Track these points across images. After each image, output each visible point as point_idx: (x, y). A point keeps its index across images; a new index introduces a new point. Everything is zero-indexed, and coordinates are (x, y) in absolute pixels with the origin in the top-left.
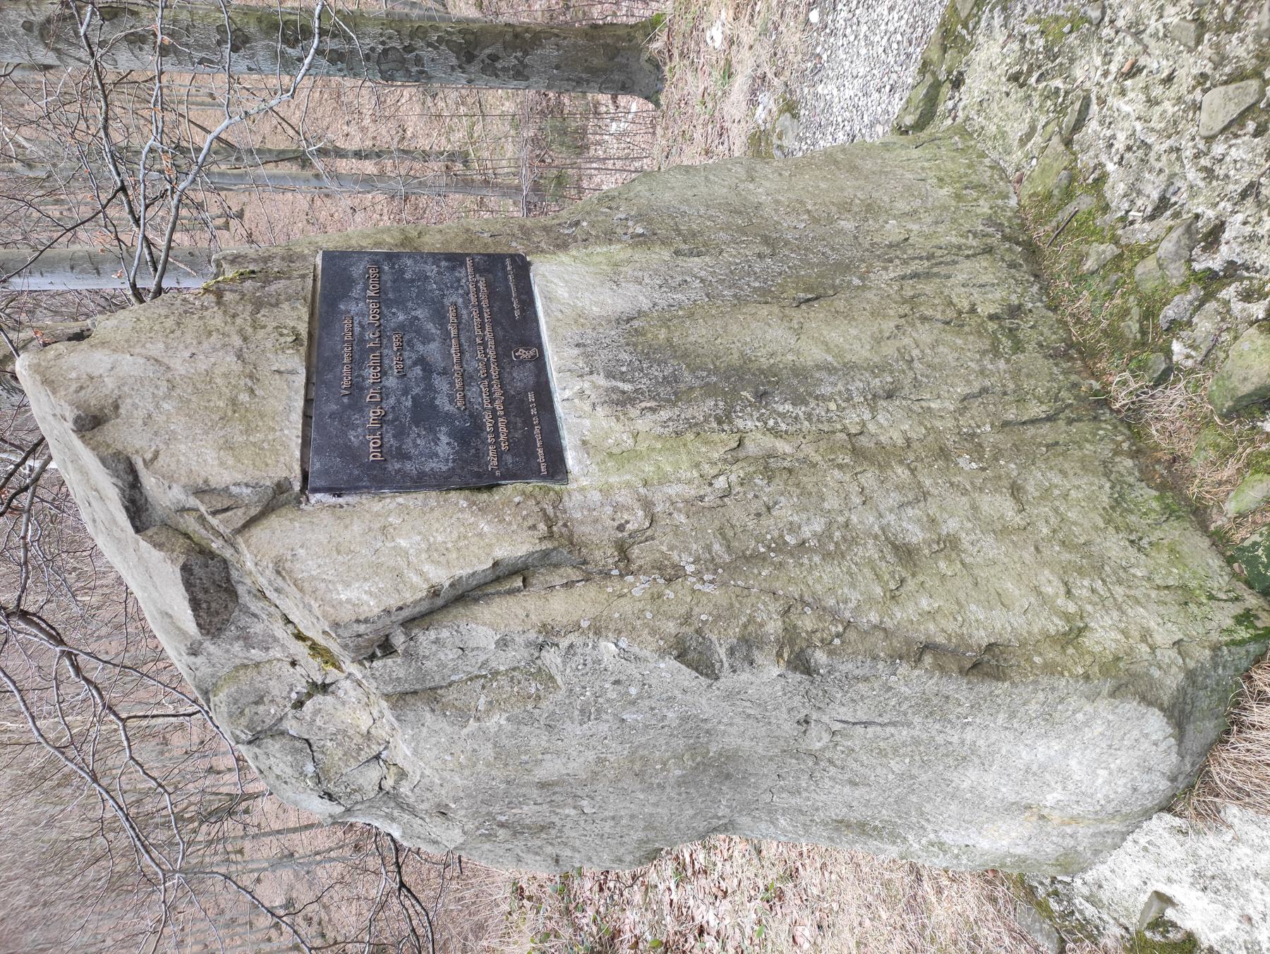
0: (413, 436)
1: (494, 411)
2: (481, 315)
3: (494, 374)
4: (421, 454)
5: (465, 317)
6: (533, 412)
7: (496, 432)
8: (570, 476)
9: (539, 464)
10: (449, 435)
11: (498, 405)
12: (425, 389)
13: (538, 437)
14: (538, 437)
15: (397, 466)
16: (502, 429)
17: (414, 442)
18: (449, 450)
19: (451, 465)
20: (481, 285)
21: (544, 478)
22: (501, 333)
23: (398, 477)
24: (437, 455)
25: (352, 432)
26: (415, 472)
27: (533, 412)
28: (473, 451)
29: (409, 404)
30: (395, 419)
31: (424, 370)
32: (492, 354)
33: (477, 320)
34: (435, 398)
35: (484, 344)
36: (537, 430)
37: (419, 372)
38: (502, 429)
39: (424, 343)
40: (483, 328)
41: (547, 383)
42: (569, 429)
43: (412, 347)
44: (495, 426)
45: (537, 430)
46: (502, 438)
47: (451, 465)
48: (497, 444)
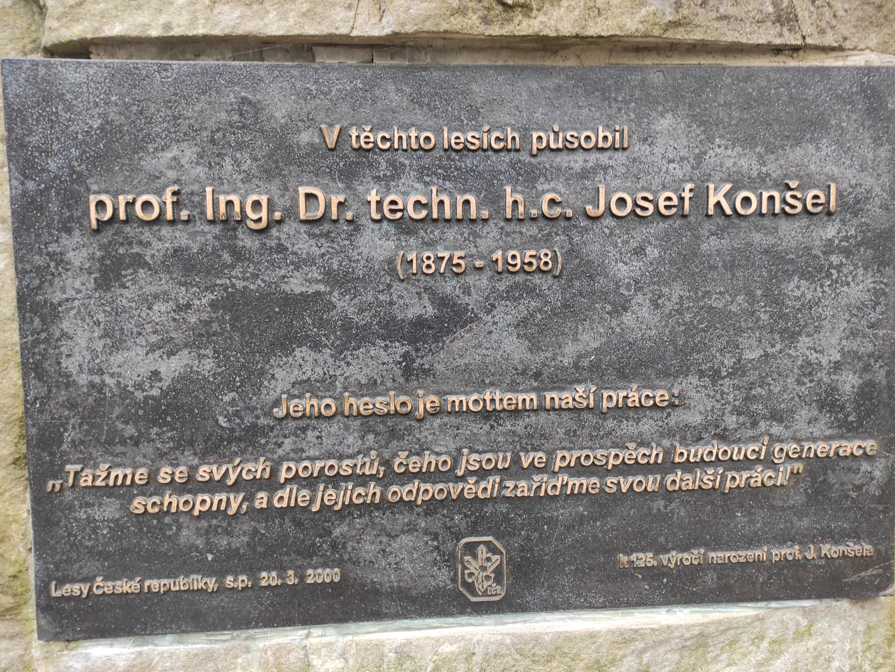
0: (183, 295)
1: (271, 484)
2: (624, 469)
3: (400, 491)
4: (117, 312)
5: (628, 427)
6: (269, 578)
7: (190, 486)
8: (56, 646)
9: (90, 579)
10: (186, 379)
11: (284, 498)
12: (347, 325)
13: (181, 584)
14: (181, 584)
15: (77, 258)
16: (203, 502)
17: (165, 296)
18: (130, 377)
19: (83, 379)
20: (759, 476)
21: (42, 590)
22: (563, 513)
23: (39, 261)
24: (117, 346)
25: (189, 153)
26: (57, 297)
27: (269, 578)
28: (130, 430)
29: (296, 285)
30: (239, 255)
31: (420, 323)
32: (471, 488)
33: (611, 457)
34: (316, 346)
35: (516, 471)
36: (197, 582)
37: (412, 313)
38: (203, 502)
39: (523, 323)
40: (578, 470)
41: (376, 616)
42: (210, 656)
43: (510, 295)
44: (211, 486)
45: (197, 582)
46: (173, 501)
47: (83, 379)
48: (152, 486)
